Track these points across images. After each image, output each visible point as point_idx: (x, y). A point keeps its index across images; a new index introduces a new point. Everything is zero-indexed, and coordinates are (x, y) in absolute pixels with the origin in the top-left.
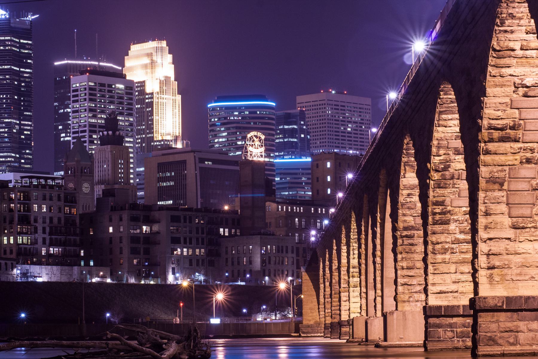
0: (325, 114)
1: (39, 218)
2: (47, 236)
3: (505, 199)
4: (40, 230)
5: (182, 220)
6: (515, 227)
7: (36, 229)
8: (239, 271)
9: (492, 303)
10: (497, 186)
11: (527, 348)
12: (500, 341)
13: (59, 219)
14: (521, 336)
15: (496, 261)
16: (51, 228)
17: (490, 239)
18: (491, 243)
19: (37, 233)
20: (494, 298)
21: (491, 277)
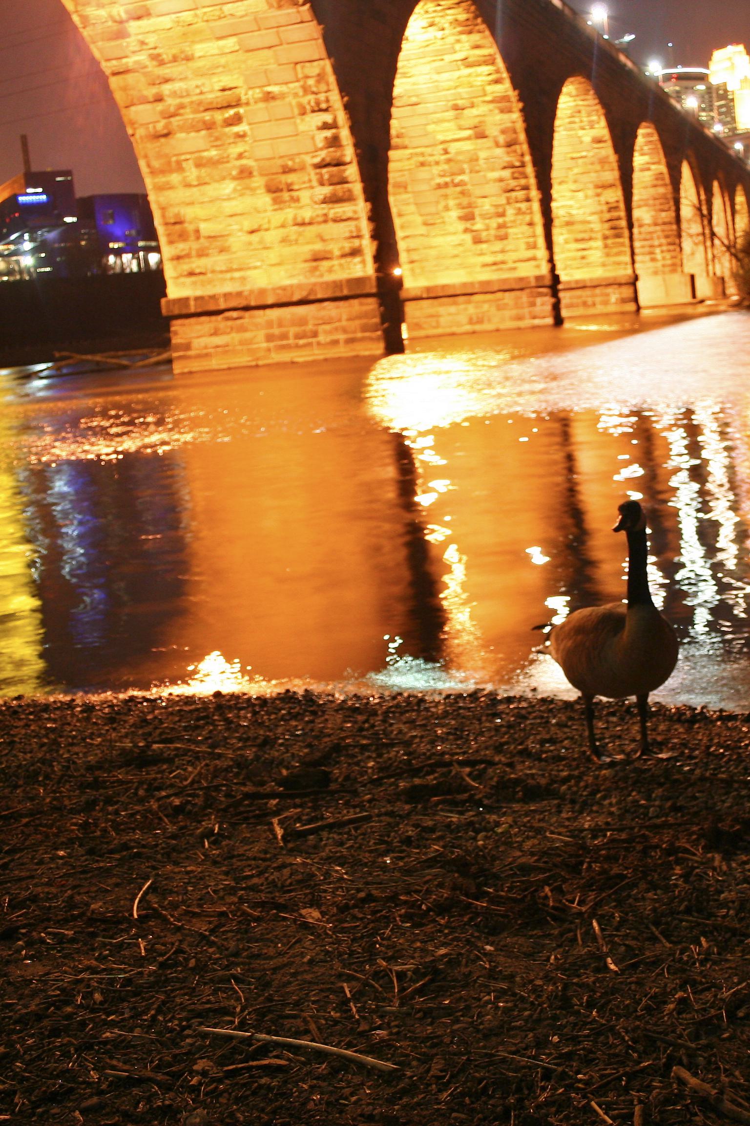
3: (411, 200)
6: (426, 224)
9: (418, 293)
10: (402, 190)
11: (448, 330)
12: (425, 326)
14: (442, 320)
15: (415, 256)
17: (407, 237)
18: (408, 240)
20: (414, 288)
21: (412, 270)
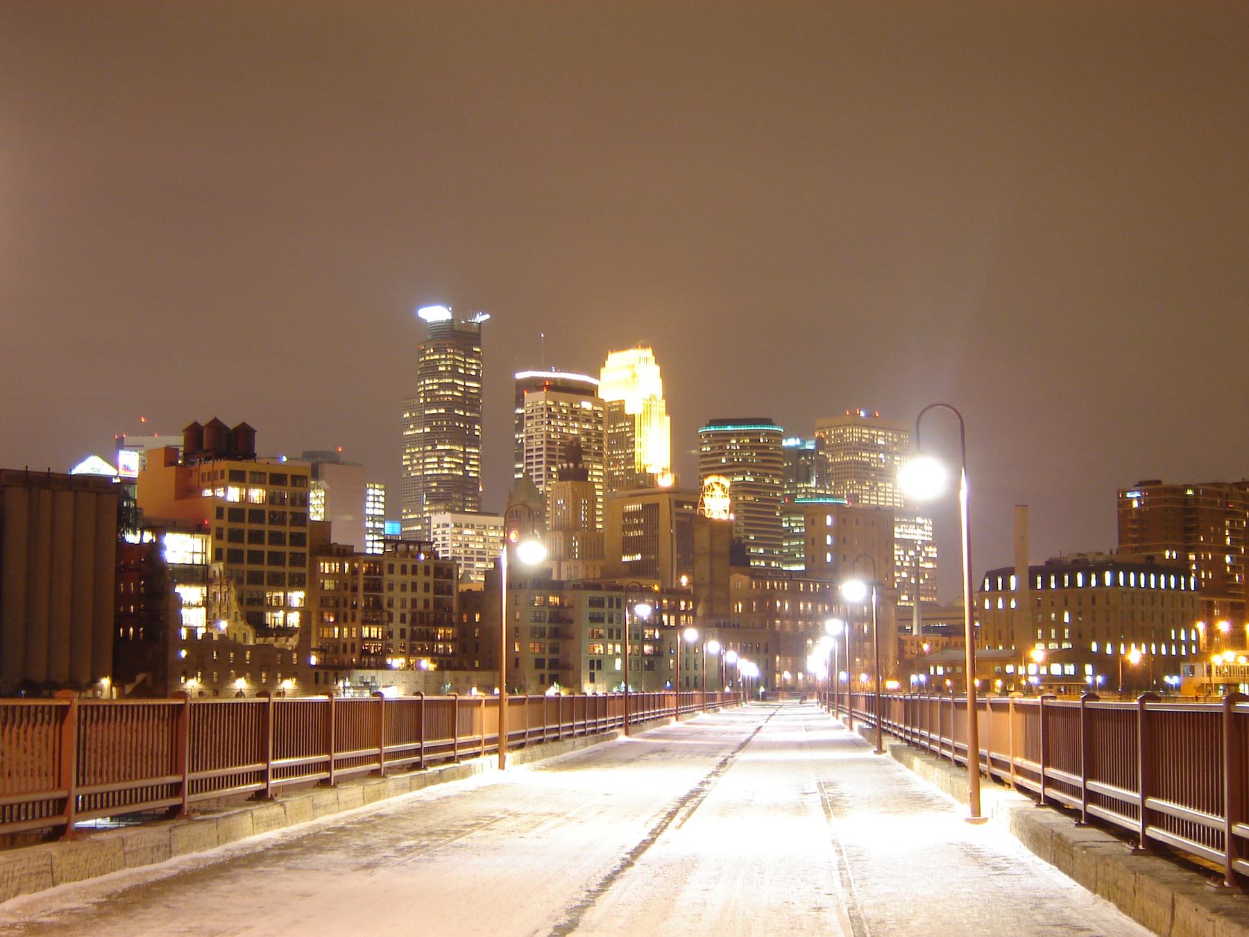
0: (414, 562)
1: (394, 601)
2: (407, 626)
4: (397, 618)
5: (607, 604)
7: (391, 616)
8: (687, 678)
13: (426, 603)
16: (413, 615)
19: (392, 622)
